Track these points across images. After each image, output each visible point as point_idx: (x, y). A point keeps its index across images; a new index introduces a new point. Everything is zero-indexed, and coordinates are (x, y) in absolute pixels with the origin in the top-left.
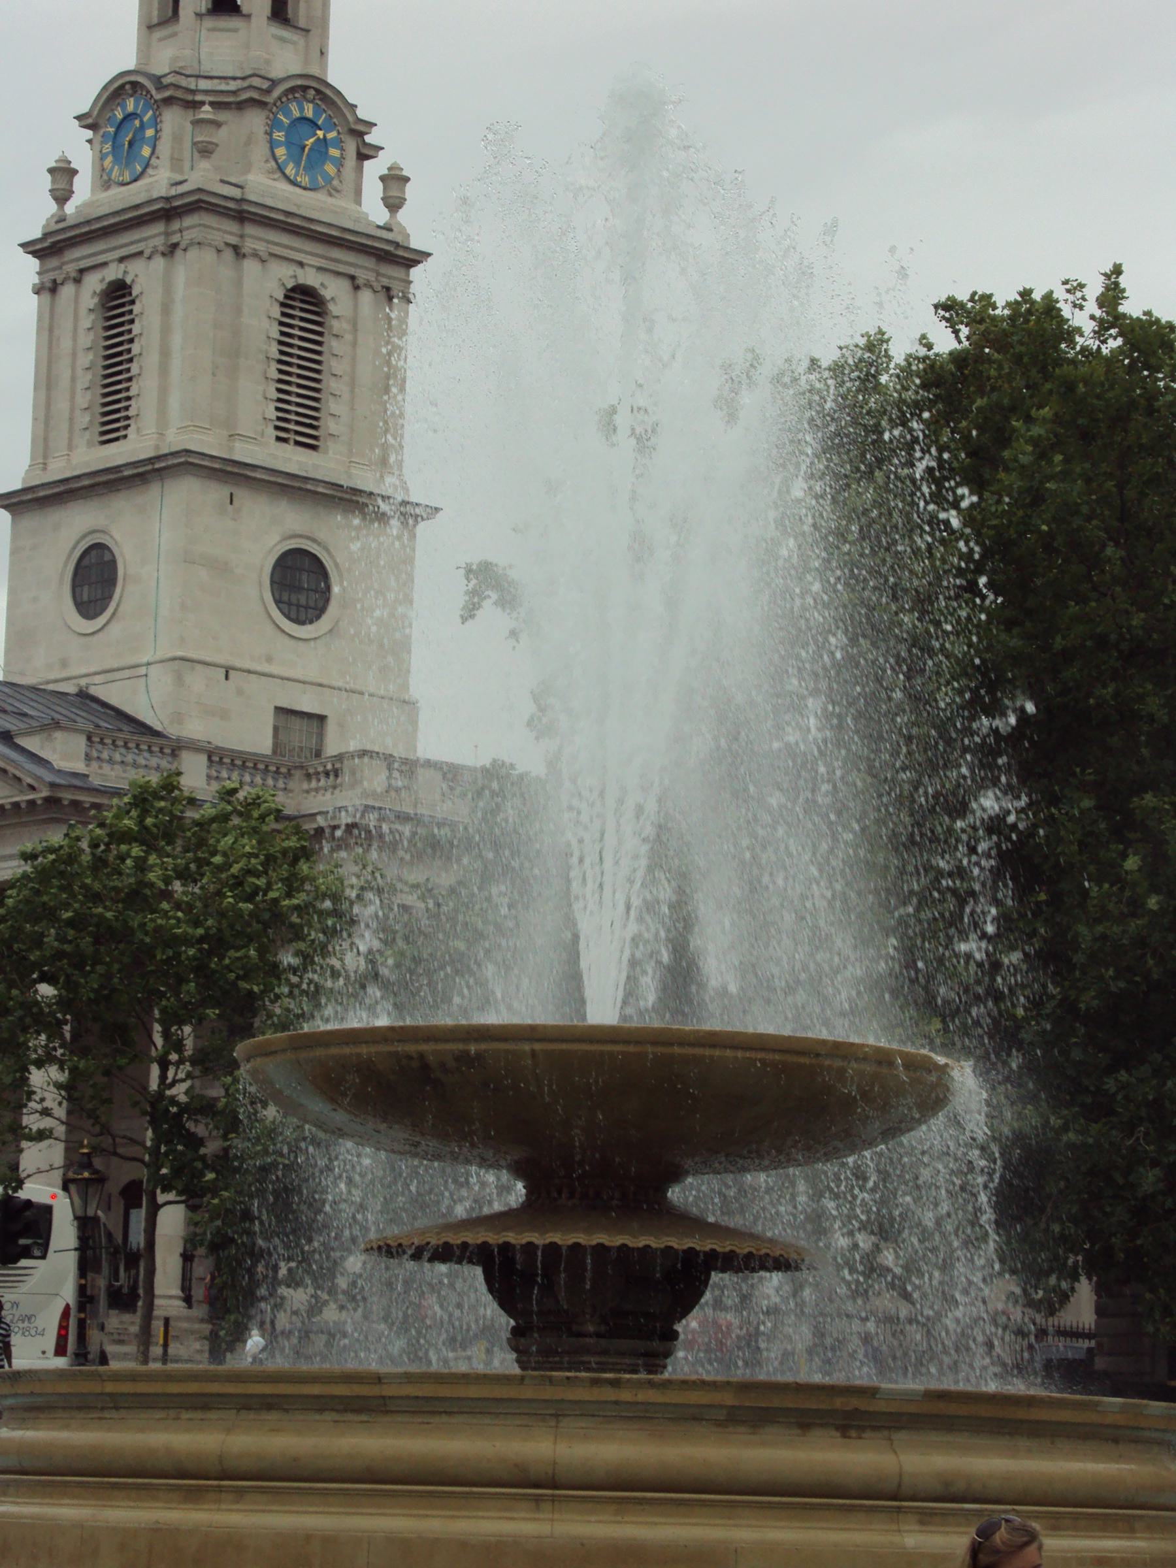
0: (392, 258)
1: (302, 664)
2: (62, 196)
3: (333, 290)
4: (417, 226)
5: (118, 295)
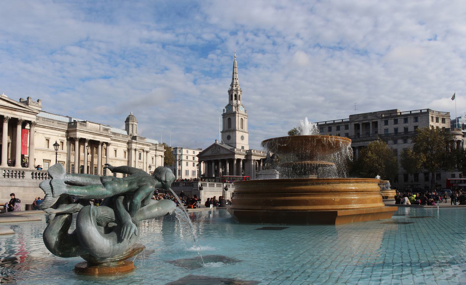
3: (243, 118)
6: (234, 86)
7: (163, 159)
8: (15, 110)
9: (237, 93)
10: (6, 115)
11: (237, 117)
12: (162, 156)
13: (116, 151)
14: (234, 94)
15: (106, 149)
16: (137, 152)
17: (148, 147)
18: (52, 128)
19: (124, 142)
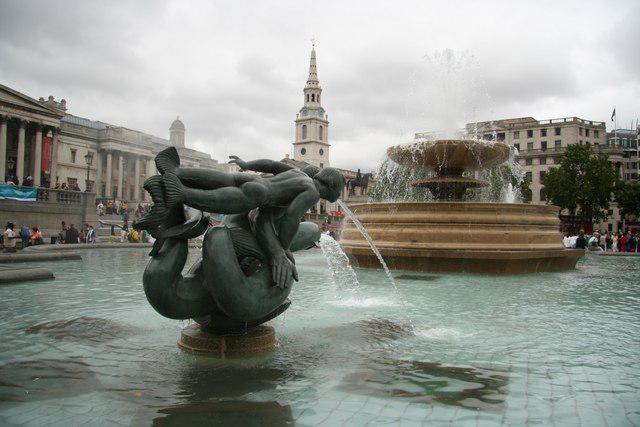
0: (327, 123)
1: (321, 159)
4: (329, 120)
8: (35, 112)
10: (24, 118)
15: (145, 165)
18: (79, 137)
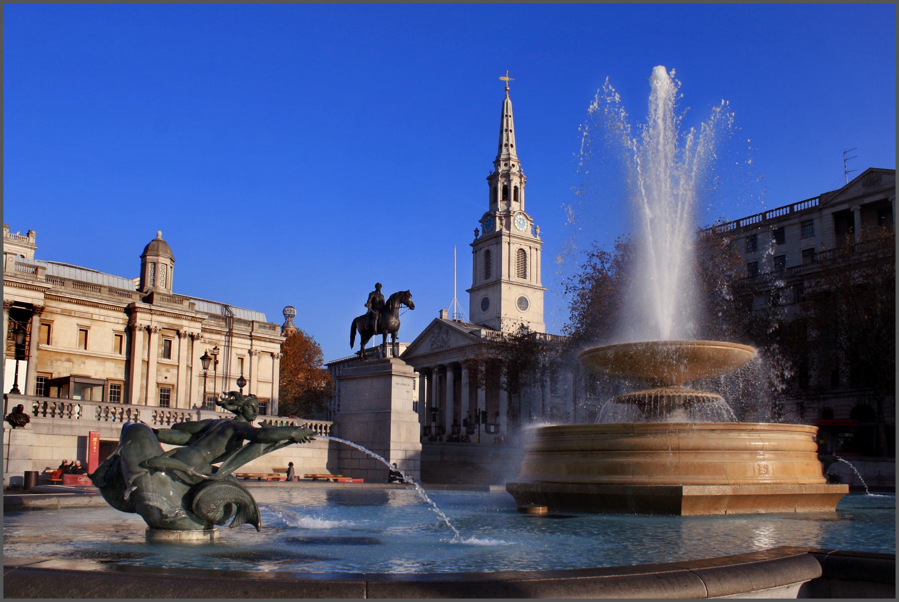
2: (477, 235)
3: (527, 250)
5: (488, 253)
6: (502, 163)
7: (277, 362)
9: (510, 181)
11: (505, 246)
12: (272, 355)
13: (85, 331)
14: (500, 186)
16: (155, 337)
17: (199, 325)
19: (115, 309)
